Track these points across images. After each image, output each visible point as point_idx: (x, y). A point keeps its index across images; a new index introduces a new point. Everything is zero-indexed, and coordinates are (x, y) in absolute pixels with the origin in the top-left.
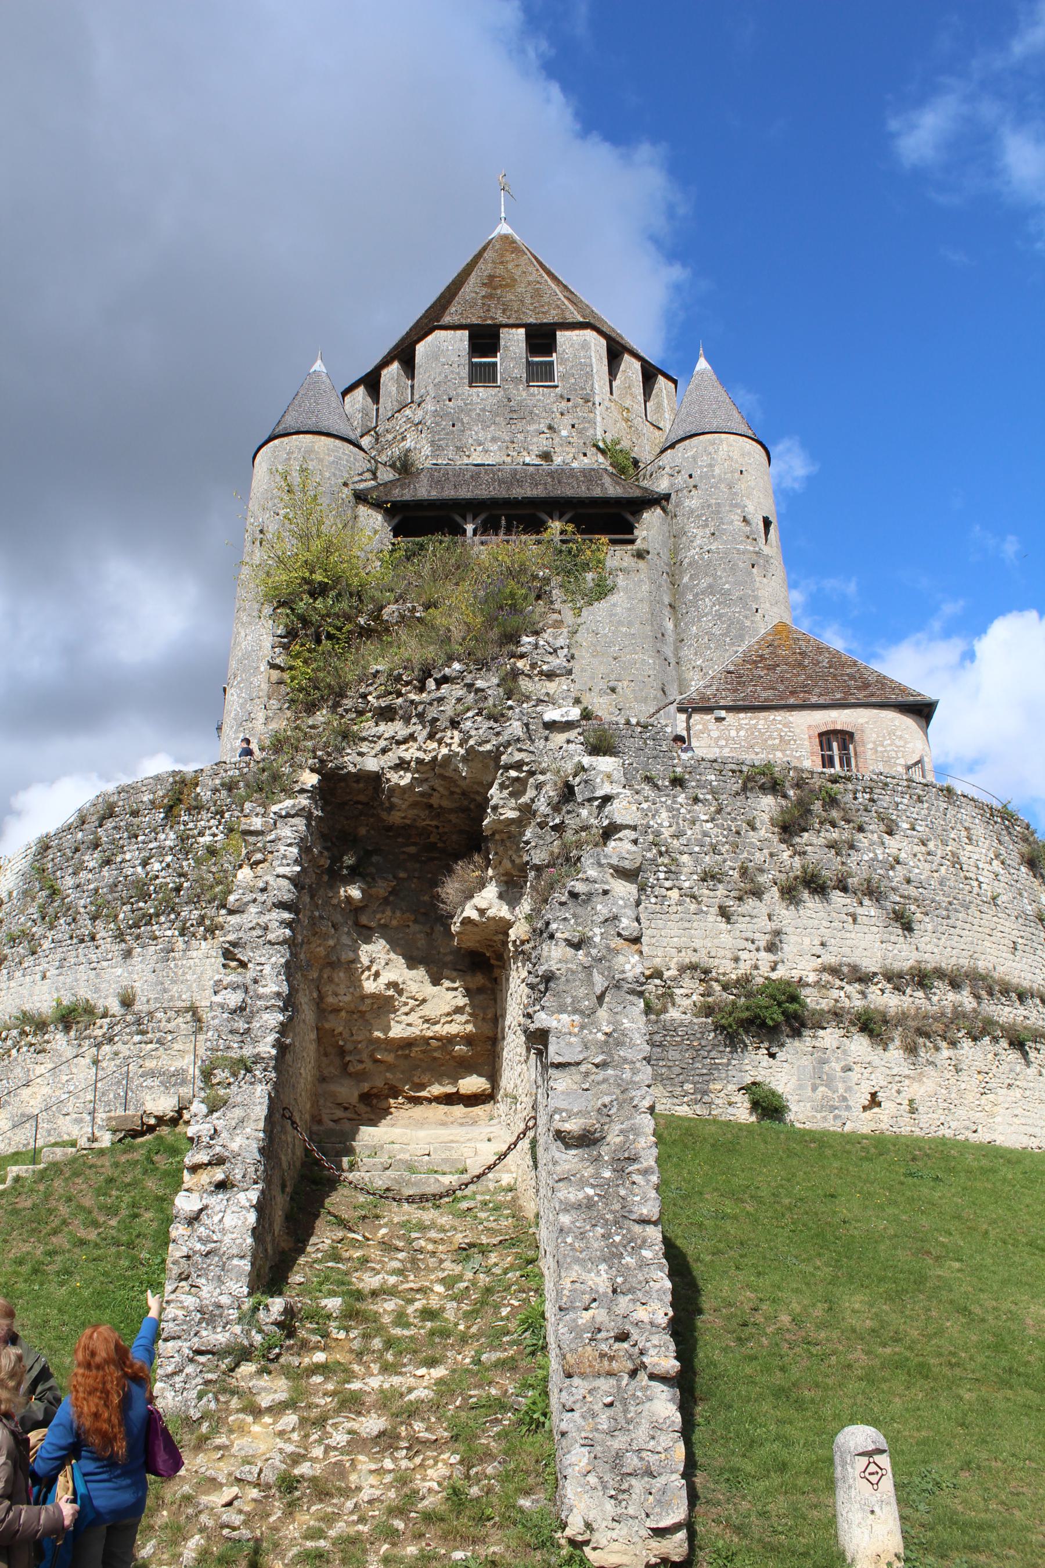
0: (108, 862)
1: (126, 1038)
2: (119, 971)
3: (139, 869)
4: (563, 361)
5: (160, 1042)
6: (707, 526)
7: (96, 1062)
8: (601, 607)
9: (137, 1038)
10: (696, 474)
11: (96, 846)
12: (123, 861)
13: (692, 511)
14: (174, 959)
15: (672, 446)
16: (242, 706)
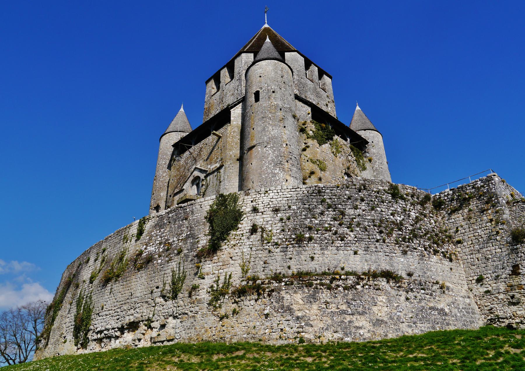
0: (373, 209)
1: (419, 291)
2: (402, 260)
3: (392, 217)
4: (327, 86)
5: (431, 295)
6: (379, 160)
7: (407, 299)
8: (364, 172)
9: (423, 291)
10: (375, 142)
11: (362, 200)
12: (382, 211)
13: (374, 153)
14: (426, 260)
15: (365, 130)
16: (277, 157)
